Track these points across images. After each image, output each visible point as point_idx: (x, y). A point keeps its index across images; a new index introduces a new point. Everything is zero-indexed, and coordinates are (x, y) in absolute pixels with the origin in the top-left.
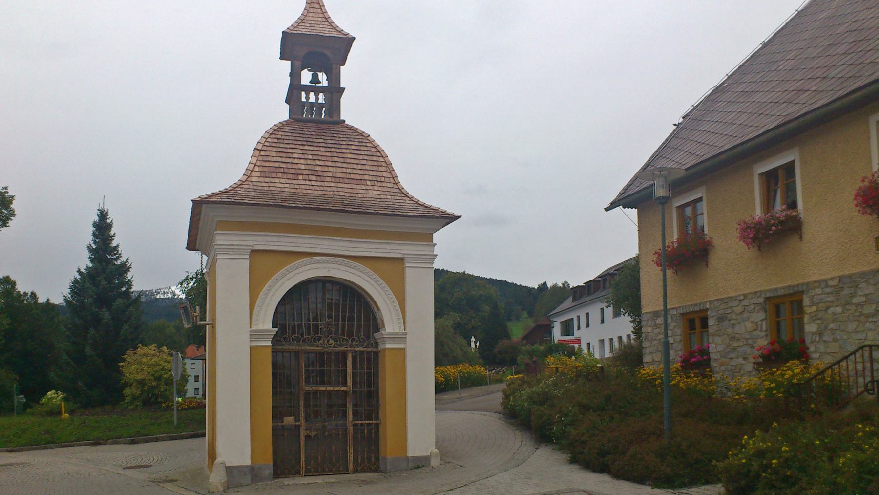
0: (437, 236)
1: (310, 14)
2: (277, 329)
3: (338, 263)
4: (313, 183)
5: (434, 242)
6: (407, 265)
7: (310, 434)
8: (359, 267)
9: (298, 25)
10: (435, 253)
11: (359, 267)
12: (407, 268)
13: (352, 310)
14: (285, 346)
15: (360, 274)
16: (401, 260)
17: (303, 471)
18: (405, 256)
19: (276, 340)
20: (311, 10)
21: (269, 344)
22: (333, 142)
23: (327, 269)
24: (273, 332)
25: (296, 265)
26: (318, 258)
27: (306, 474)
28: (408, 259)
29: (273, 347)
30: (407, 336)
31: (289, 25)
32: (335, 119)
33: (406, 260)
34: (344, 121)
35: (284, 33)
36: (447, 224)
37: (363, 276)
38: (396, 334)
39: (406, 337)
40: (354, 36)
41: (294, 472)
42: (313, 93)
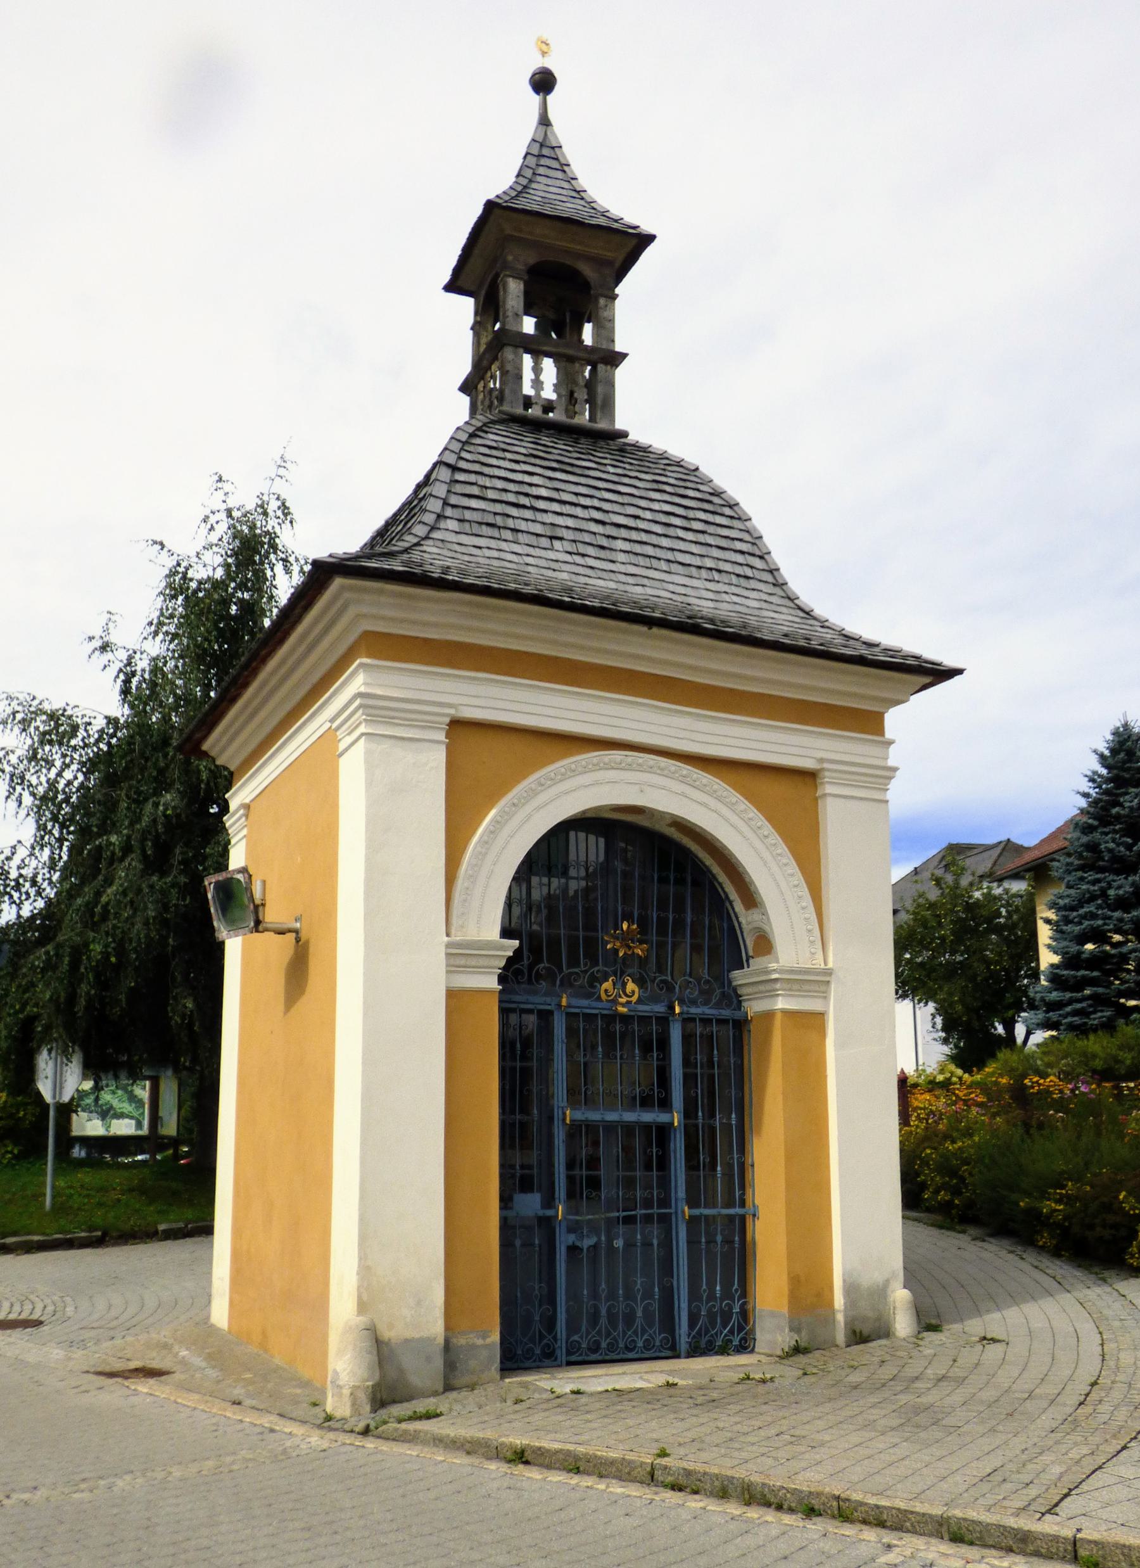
0: (895, 719)
1: (539, 179)
2: (516, 943)
3: (666, 772)
4: (591, 562)
5: (889, 735)
6: (829, 789)
7: (578, 1244)
8: (716, 787)
9: (517, 196)
10: (891, 763)
11: (716, 787)
12: (829, 800)
13: (680, 908)
14: (517, 994)
15: (712, 802)
16: (809, 777)
17: (561, 1354)
18: (826, 765)
19: (511, 973)
20: (541, 170)
21: (491, 983)
22: (619, 471)
23: (637, 787)
24: (502, 948)
25: (563, 770)
26: (617, 755)
27: (573, 1358)
28: (834, 775)
29: (506, 997)
30: (833, 979)
31: (499, 192)
32: (602, 425)
33: (827, 777)
34: (625, 434)
35: (490, 206)
36: (925, 687)
37: (725, 811)
38: (807, 971)
39: (828, 982)
40: (652, 231)
41: (538, 1351)
42: (585, 343)
